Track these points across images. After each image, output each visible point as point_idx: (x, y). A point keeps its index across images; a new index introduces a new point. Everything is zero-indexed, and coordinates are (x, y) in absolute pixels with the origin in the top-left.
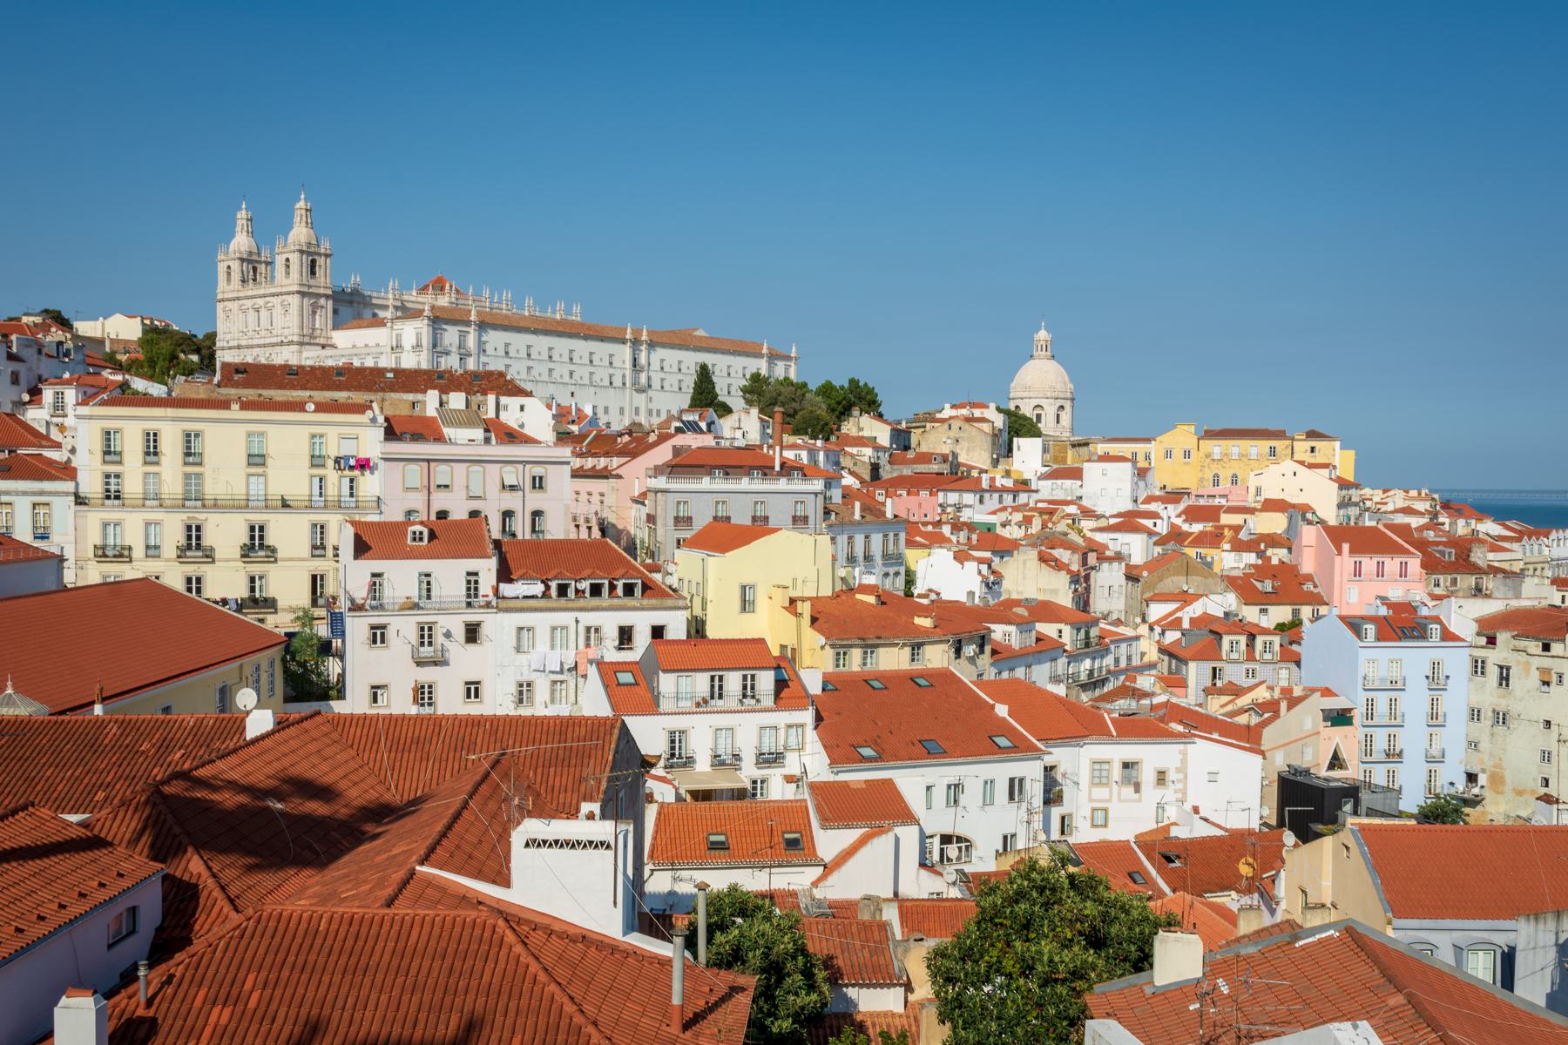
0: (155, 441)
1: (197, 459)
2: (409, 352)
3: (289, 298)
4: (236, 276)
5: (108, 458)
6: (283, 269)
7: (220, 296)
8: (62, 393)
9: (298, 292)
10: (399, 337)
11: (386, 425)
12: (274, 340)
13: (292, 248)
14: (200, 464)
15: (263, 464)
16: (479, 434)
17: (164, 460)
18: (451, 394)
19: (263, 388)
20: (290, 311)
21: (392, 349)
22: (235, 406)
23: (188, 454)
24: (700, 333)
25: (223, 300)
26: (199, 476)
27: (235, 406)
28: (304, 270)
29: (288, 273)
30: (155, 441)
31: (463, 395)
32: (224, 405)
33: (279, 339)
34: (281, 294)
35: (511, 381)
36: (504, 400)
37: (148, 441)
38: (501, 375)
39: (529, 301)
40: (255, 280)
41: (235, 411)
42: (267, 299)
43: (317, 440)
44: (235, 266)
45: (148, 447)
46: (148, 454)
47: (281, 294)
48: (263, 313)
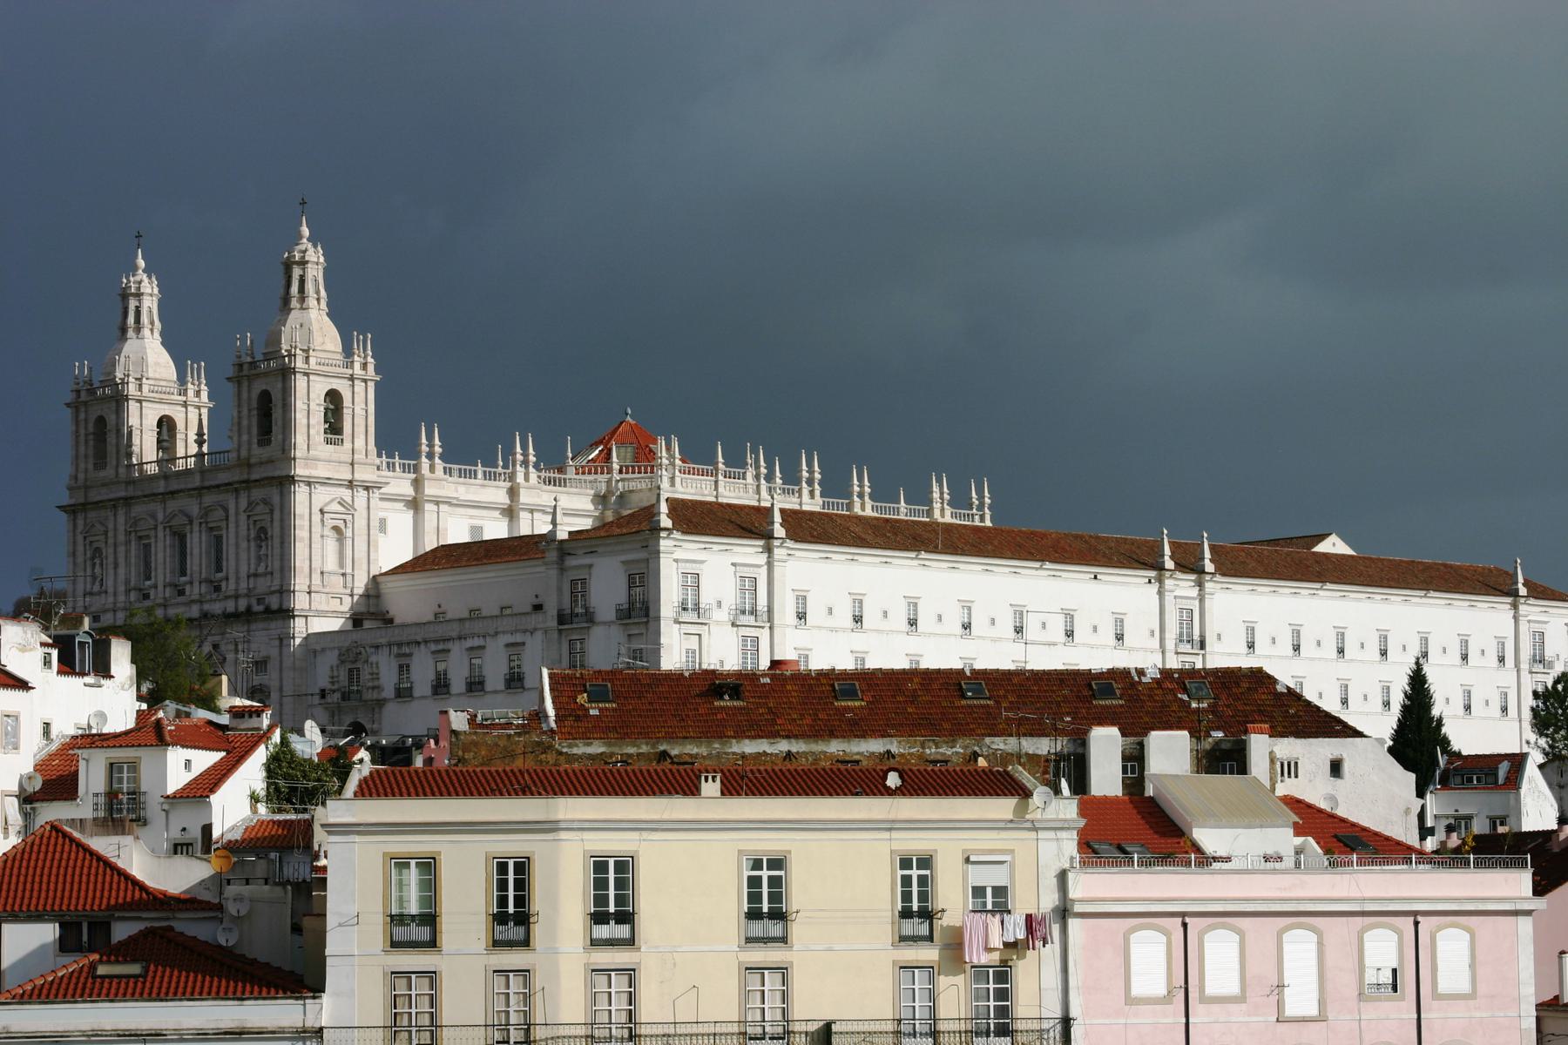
0: (521, 885)
1: (622, 931)
2: (608, 624)
5: (400, 933)
10: (579, 588)
11: (1082, 823)
12: (230, 606)
14: (630, 942)
15: (784, 940)
16: (1284, 839)
17: (538, 931)
18: (1154, 734)
19: (671, 737)
21: (562, 619)
22: (711, 788)
23: (599, 918)
24: (1333, 545)
26: (630, 973)
27: (711, 788)
30: (621, 884)
31: (1186, 733)
32: (683, 783)
33: (242, 605)
35: (1294, 696)
36: (1287, 747)
37: (503, 885)
38: (1259, 678)
39: (860, 484)
41: (710, 801)
42: (209, 499)
43: (915, 873)
45: (503, 901)
46: (500, 918)
48: (197, 543)
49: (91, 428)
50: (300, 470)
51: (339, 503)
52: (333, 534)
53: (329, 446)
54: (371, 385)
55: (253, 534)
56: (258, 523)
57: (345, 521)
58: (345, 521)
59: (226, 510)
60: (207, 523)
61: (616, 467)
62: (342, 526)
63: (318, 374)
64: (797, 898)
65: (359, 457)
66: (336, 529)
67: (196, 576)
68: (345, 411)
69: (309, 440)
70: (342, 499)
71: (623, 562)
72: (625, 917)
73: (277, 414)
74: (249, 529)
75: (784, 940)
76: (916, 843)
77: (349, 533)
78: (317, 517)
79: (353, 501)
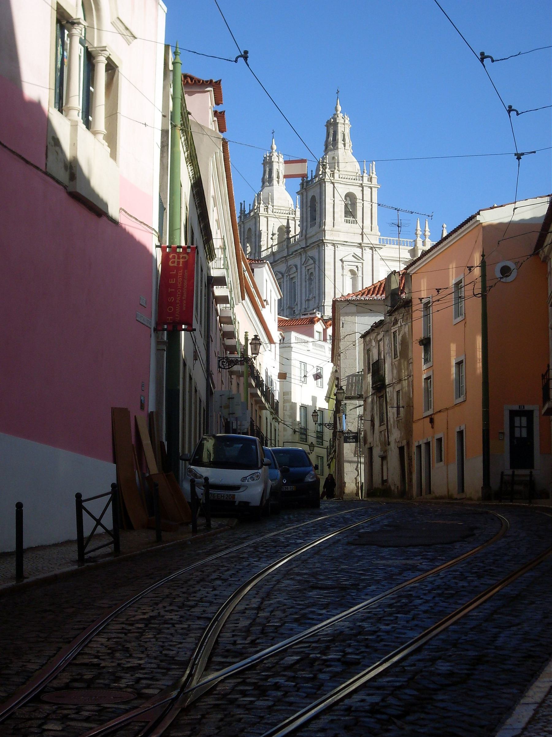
50: (328, 236)
51: (353, 256)
52: (349, 274)
53: (348, 224)
54: (375, 191)
56: (310, 270)
57: (357, 267)
58: (357, 267)
59: (296, 266)
60: (289, 275)
62: (356, 269)
63: (340, 183)
65: (367, 230)
66: (352, 271)
67: (285, 306)
68: (358, 204)
69: (334, 220)
70: (354, 253)
73: (318, 206)
74: (306, 275)
77: (360, 274)
78: (339, 264)
79: (362, 255)
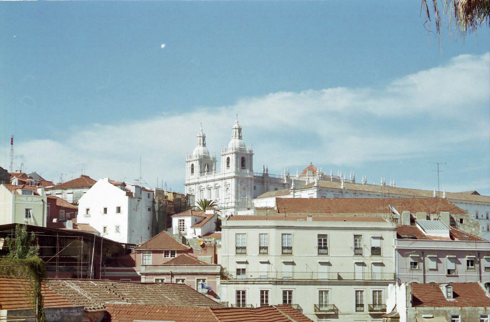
1: (289, 251)
3: (229, 181)
4: (197, 169)
6: (226, 164)
7: (187, 182)
8: (183, 220)
9: (234, 177)
13: (231, 151)
20: (230, 188)
23: (283, 248)
25: (189, 184)
28: (239, 163)
29: (228, 166)
34: (225, 179)
40: (208, 172)
42: (216, 182)
44: (196, 164)
47: (225, 179)
48: (213, 191)
49: (190, 167)
55: (226, 189)
61: (307, 175)
64: (330, 243)
71: (309, 194)
72: (291, 248)
75: (327, 254)
76: (357, 233)
